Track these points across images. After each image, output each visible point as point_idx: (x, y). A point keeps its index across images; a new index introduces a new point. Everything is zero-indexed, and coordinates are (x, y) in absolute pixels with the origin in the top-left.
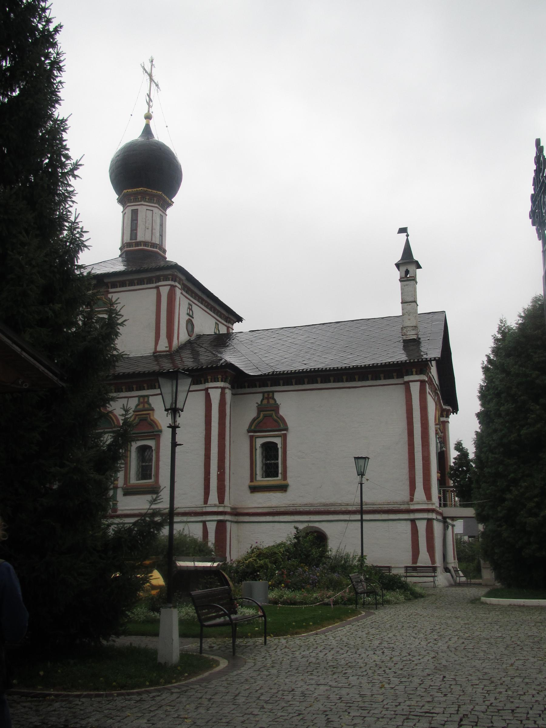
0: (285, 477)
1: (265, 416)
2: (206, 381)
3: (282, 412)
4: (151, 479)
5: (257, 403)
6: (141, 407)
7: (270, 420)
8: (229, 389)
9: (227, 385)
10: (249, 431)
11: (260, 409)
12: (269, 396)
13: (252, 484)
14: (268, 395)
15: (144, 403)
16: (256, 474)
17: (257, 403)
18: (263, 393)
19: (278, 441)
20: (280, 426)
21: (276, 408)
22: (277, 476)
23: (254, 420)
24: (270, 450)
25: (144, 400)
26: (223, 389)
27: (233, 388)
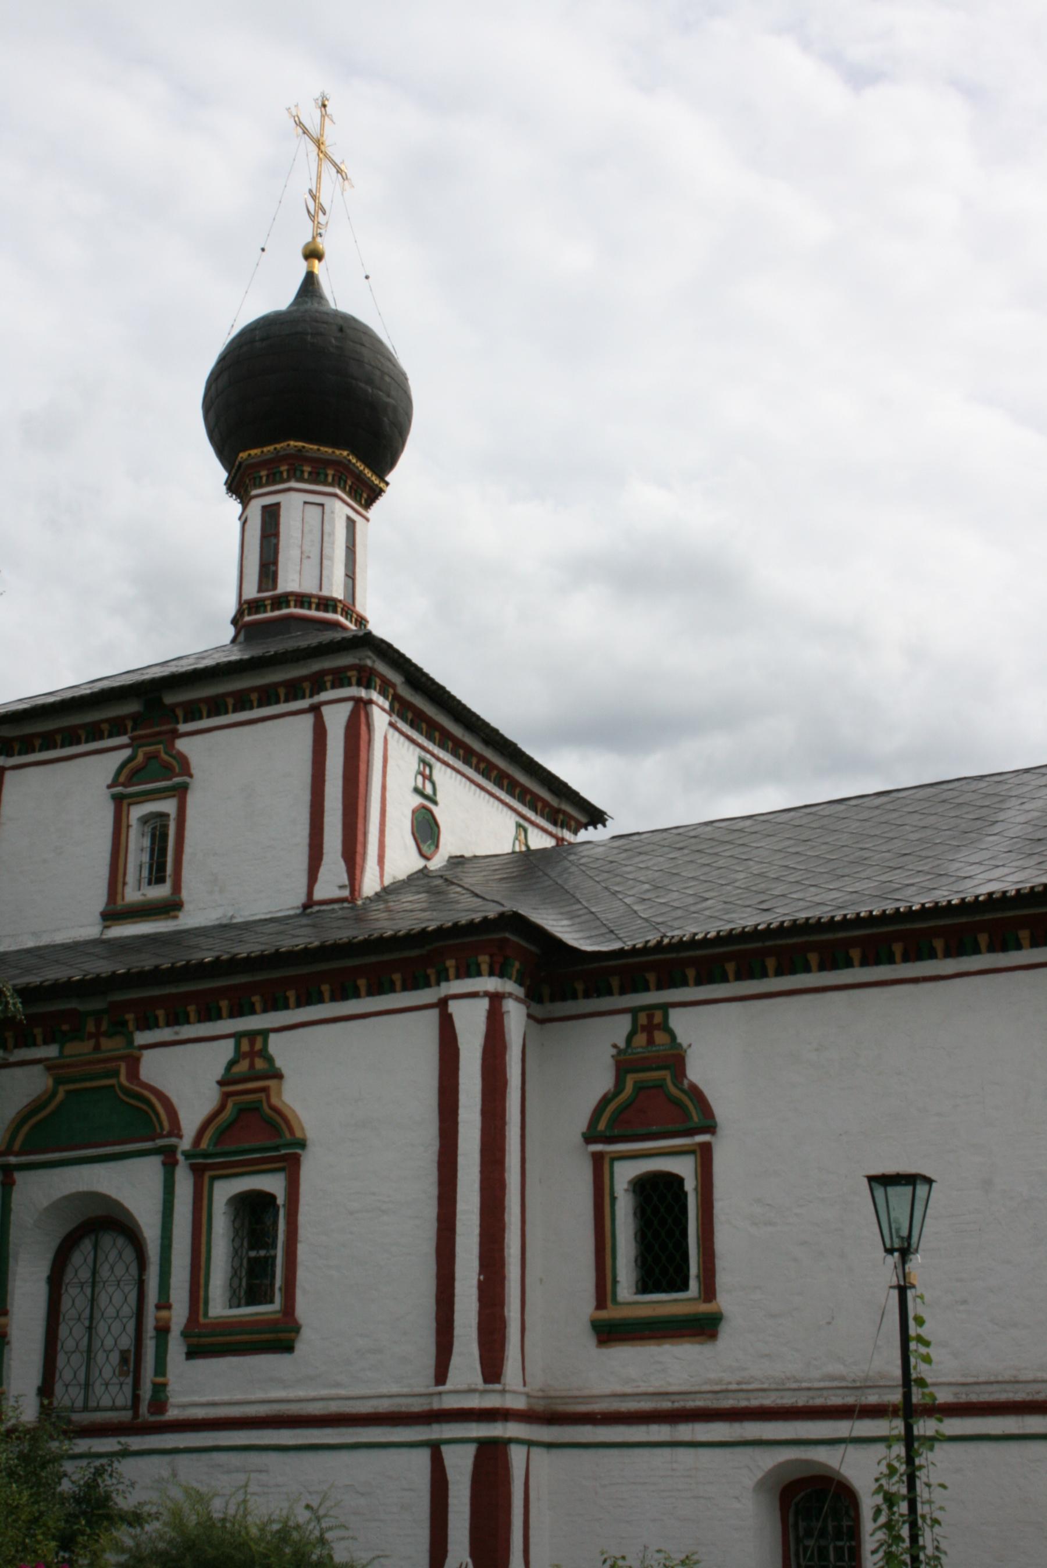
0: (709, 1291)
1: (640, 1088)
2: (443, 976)
3: (696, 1073)
4: (272, 1302)
5: (615, 1046)
6: (243, 1066)
7: (655, 1100)
8: (517, 999)
9: (508, 986)
10: (589, 1138)
11: (624, 1065)
12: (652, 1024)
13: (604, 1314)
14: (650, 1017)
15: (252, 1054)
16: (615, 1282)
17: (615, 1046)
18: (634, 1011)
19: (684, 1168)
20: (687, 1117)
21: (675, 1061)
22: (684, 1286)
23: (605, 1101)
24: (660, 1199)
25: (252, 1044)
26: (496, 999)
27: (533, 996)
